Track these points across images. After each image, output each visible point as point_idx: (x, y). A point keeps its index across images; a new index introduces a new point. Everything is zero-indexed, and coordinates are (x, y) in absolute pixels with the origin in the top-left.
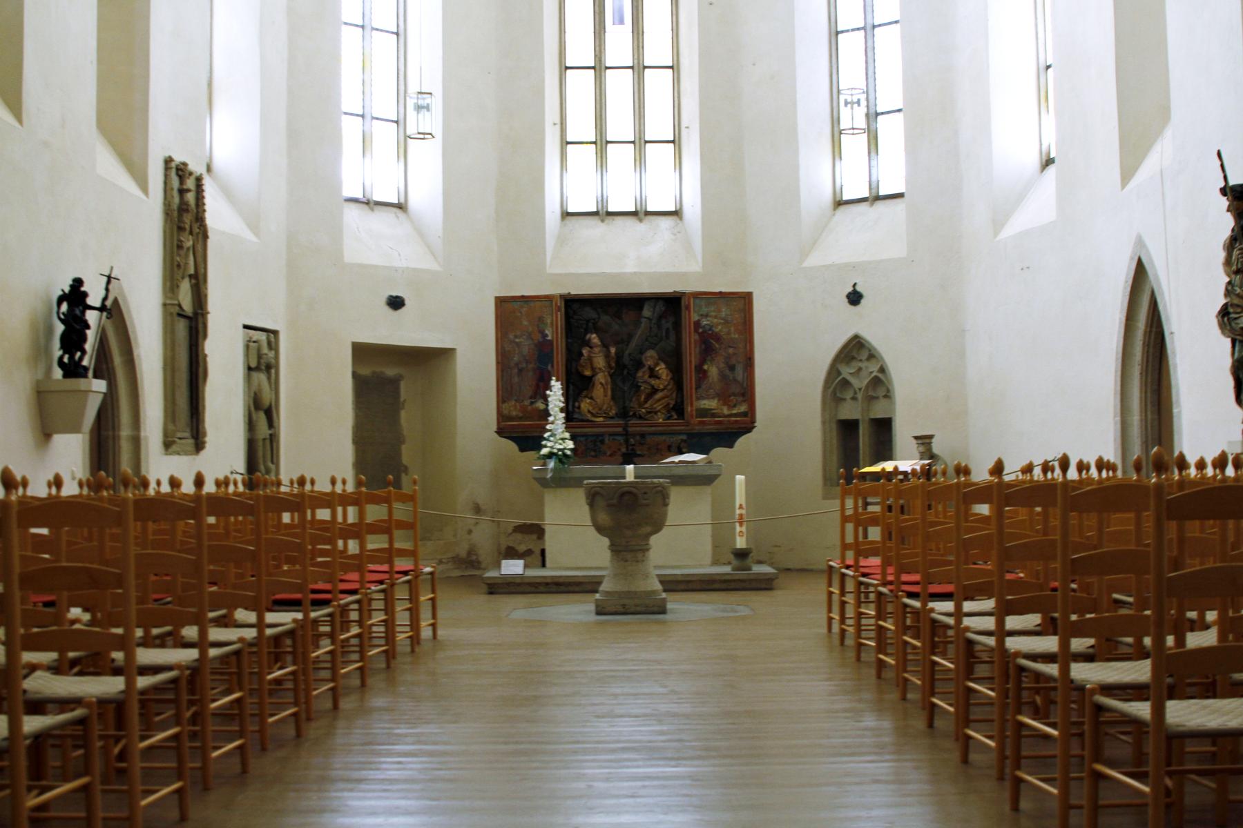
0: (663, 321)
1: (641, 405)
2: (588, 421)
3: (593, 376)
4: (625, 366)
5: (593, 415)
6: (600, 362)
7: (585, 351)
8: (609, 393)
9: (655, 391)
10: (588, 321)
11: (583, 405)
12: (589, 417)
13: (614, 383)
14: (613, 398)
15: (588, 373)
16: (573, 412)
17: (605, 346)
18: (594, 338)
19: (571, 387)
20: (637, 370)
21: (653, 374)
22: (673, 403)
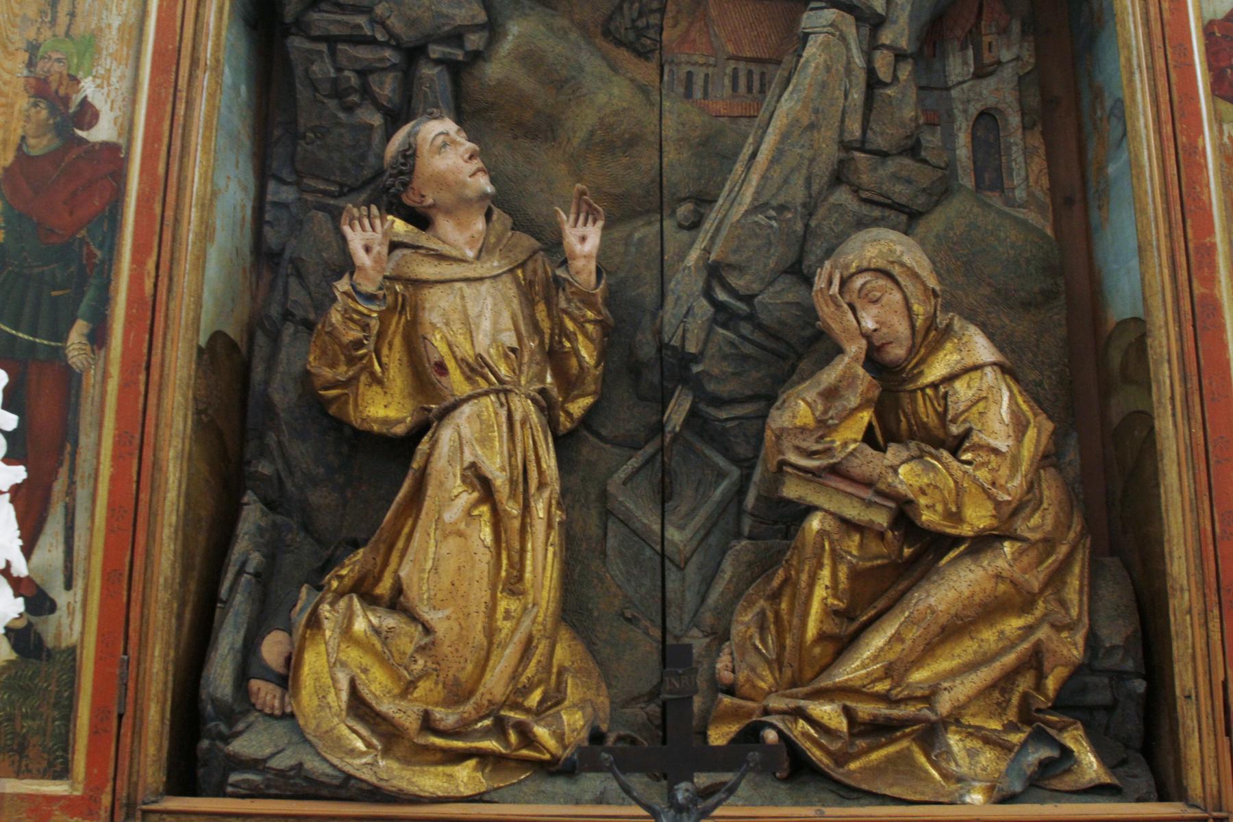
0: (957, 66)
1: (805, 673)
2: (347, 788)
3: (423, 428)
4: (677, 366)
5: (388, 734)
6: (476, 315)
7: (366, 237)
8: (543, 565)
9: (919, 547)
10: (413, 54)
11: (313, 662)
12: (358, 754)
13: (582, 492)
14: (574, 609)
15: (384, 408)
16: (242, 705)
17: (517, 211)
18: (443, 148)
19: (252, 516)
20: (769, 399)
21: (900, 407)
22: (1071, 648)
